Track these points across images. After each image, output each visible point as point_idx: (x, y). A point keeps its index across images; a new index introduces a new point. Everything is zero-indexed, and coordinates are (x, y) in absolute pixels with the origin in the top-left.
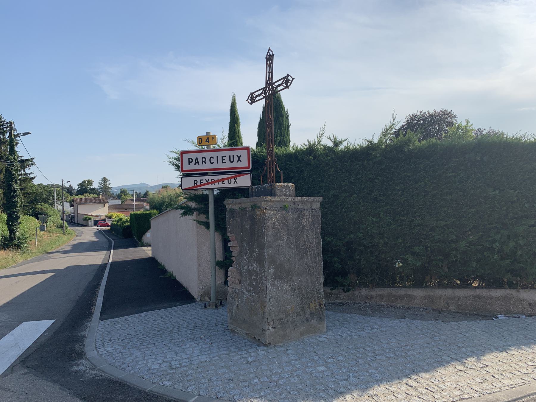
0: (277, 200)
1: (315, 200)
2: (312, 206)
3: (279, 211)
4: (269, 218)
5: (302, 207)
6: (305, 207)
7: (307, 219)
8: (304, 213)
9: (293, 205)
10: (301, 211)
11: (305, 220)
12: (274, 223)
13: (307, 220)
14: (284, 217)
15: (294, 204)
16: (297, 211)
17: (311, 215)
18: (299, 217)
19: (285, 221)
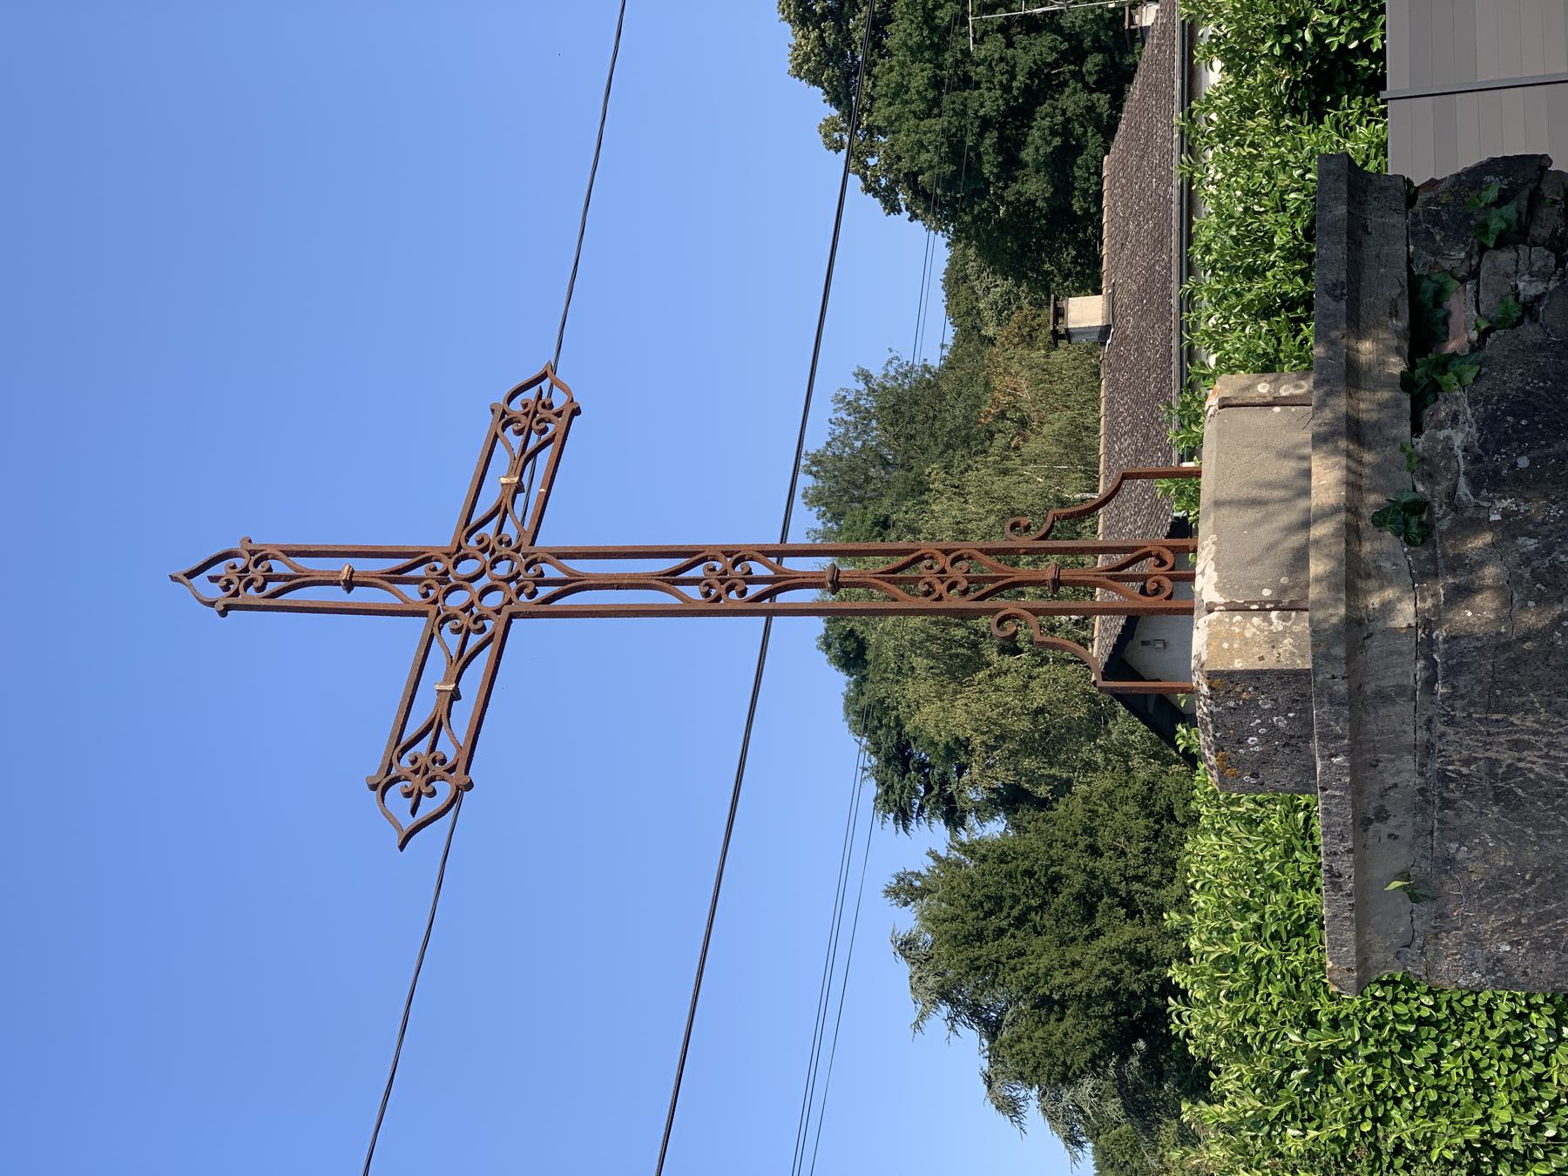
0: (1350, 935)
1: (1341, 687)
2: (1401, 690)
3: (1442, 916)
4: (1490, 971)
5: (1409, 763)
6: (1409, 739)
7: (1517, 745)
8: (1467, 762)
9: (1392, 822)
10: (1444, 778)
11: (1534, 763)
12: (1539, 947)
13: (1529, 746)
14: (1488, 887)
15: (1382, 815)
16: (1447, 804)
17: (1488, 709)
18: (1501, 797)
19: (1531, 882)
